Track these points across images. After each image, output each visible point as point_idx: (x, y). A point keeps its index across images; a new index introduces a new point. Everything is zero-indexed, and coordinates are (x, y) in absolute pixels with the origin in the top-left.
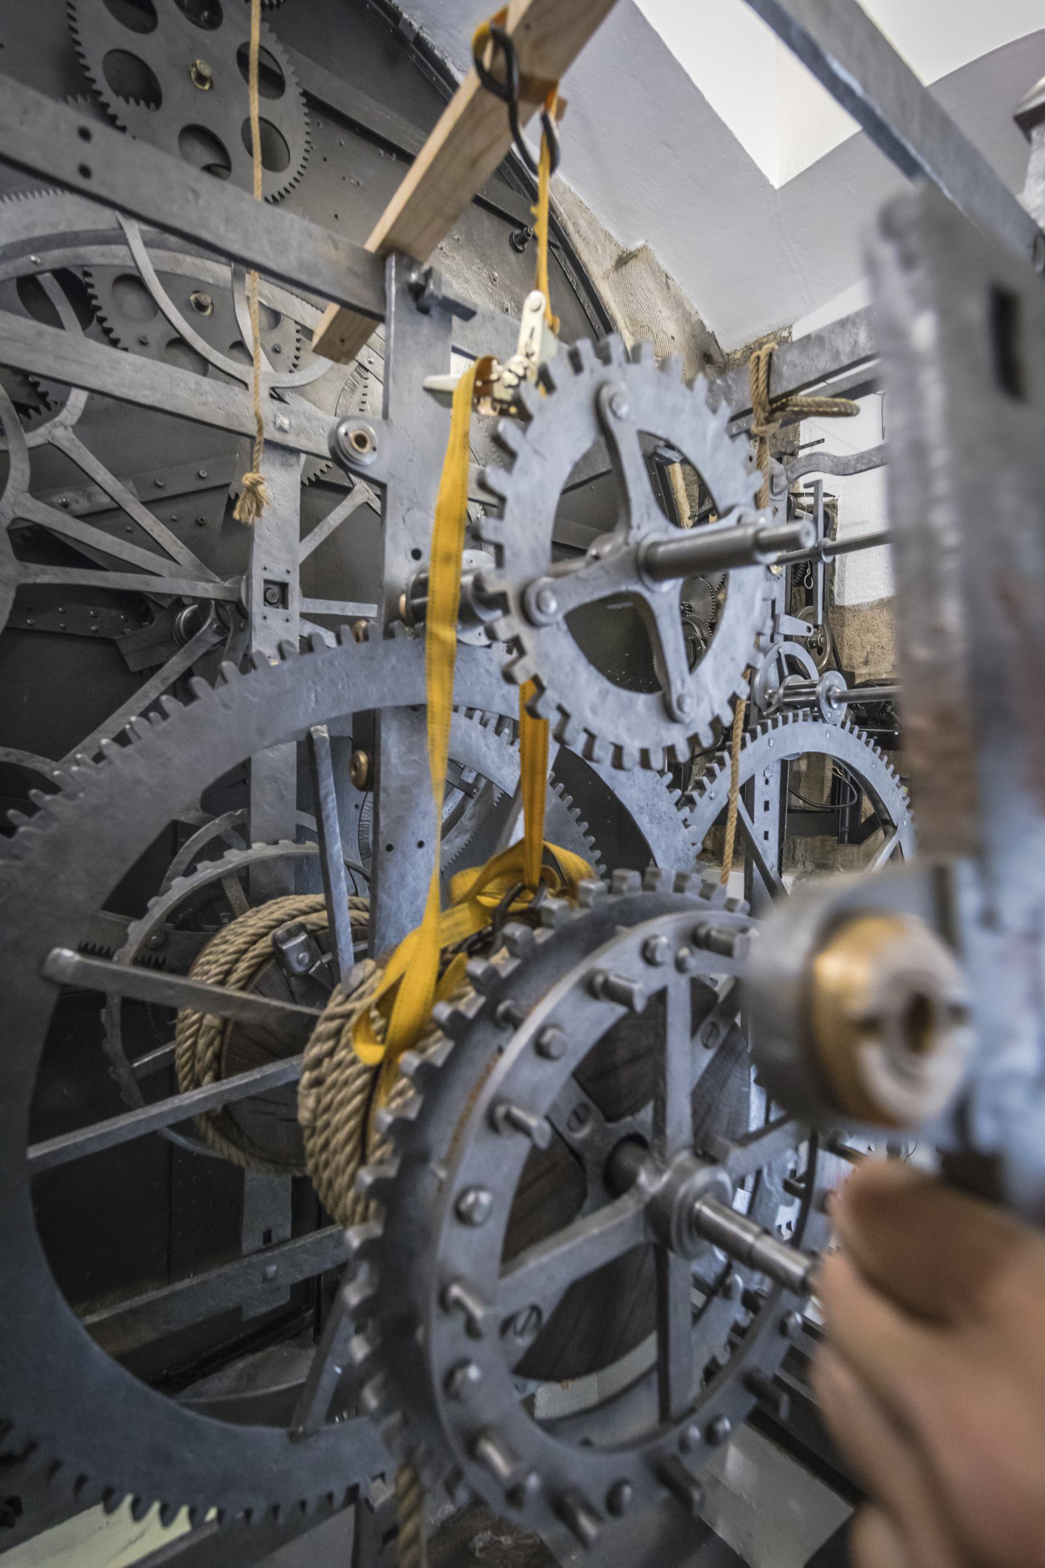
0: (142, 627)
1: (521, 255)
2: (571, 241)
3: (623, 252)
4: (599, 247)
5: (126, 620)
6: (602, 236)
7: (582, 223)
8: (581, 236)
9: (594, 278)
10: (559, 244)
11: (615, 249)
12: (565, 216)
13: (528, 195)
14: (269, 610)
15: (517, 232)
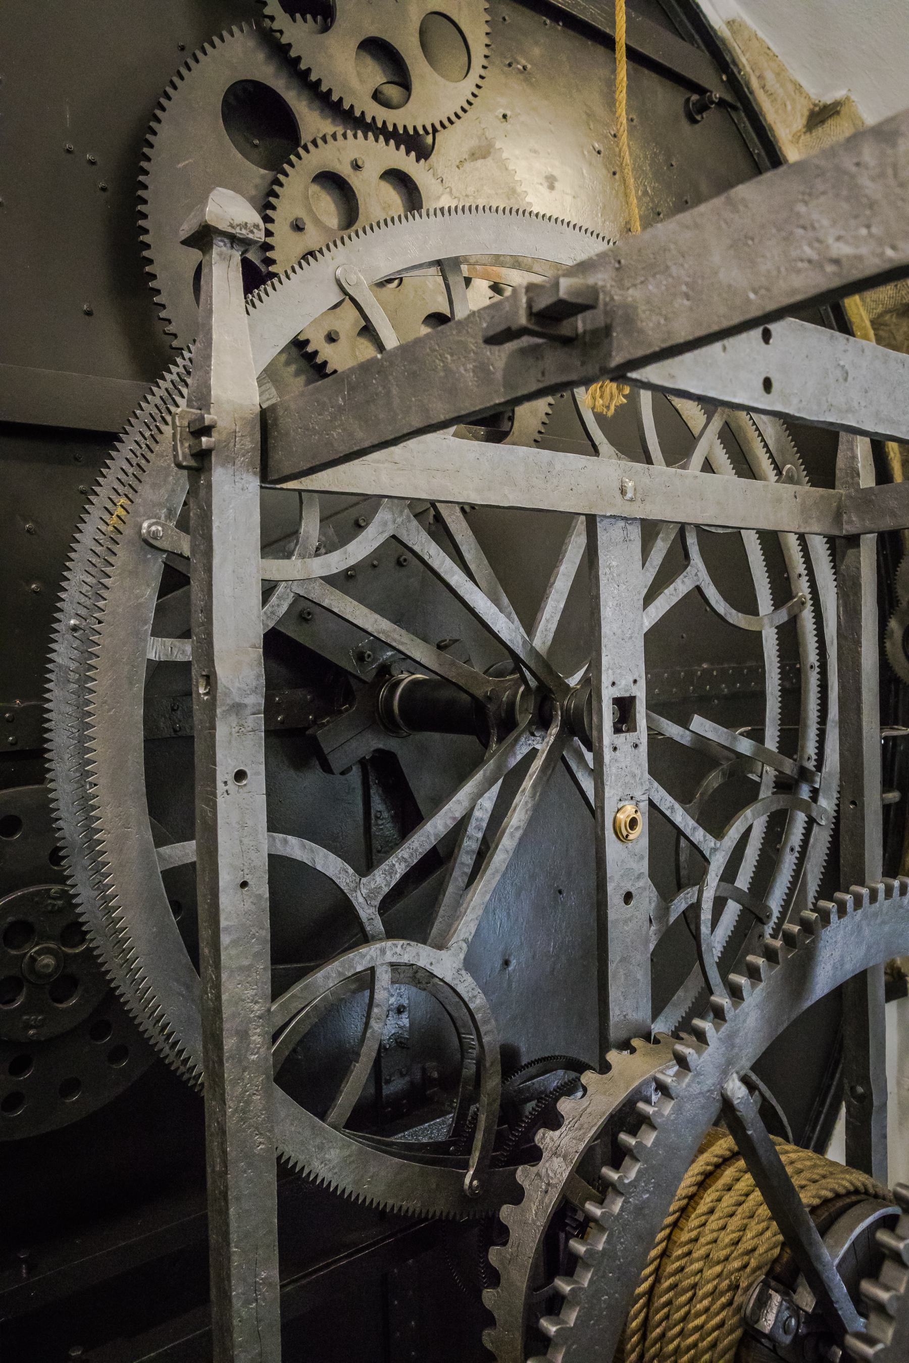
0: (340, 712)
1: (697, 126)
2: (755, 99)
3: (815, 105)
4: (788, 103)
5: (312, 701)
6: (790, 87)
7: (769, 76)
8: (766, 92)
9: (781, 144)
10: (739, 105)
11: (805, 102)
12: (748, 69)
13: (703, 48)
14: (622, 740)
15: (695, 97)
